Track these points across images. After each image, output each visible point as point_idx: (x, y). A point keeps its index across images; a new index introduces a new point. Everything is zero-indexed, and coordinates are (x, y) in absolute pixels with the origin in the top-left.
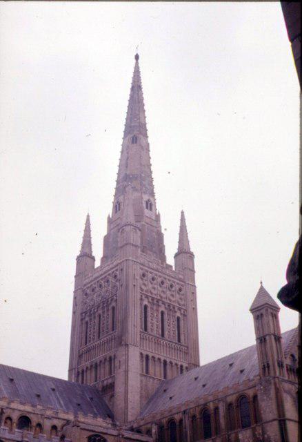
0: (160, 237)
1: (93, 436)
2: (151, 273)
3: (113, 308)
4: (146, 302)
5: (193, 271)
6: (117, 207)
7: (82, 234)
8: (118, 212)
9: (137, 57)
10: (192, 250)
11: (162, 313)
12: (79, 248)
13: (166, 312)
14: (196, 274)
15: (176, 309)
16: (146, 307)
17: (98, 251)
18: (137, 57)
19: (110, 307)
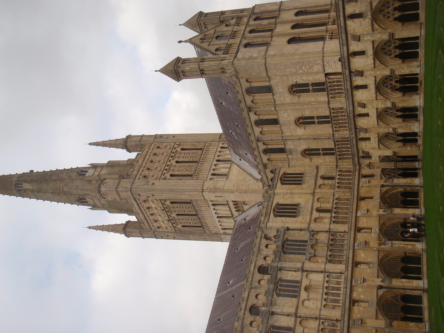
0: (112, 165)
1: (274, 214)
2: (143, 171)
3: (172, 203)
4: (168, 176)
5: (143, 136)
6: (81, 201)
7: (105, 233)
8: (88, 200)
10: (125, 137)
11: (177, 162)
12: (118, 235)
13: (176, 159)
14: (145, 134)
15: (174, 151)
16: (172, 175)
19: (171, 205)
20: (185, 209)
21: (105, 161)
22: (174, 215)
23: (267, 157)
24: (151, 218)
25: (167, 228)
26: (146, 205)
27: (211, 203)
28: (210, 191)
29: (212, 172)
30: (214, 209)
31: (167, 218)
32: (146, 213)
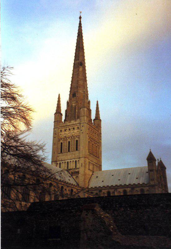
3: (77, 141)
9: (80, 18)
12: (55, 109)
16: (89, 142)
17: (63, 112)
18: (80, 18)
20: (73, 146)
21: (91, 108)
22: (69, 140)
23: (106, 193)
24: (68, 128)
25: (61, 135)
26: (76, 128)
27: (77, 160)
28: (85, 161)
29: (90, 162)
30: (73, 161)
31: (67, 136)
32: (71, 127)
